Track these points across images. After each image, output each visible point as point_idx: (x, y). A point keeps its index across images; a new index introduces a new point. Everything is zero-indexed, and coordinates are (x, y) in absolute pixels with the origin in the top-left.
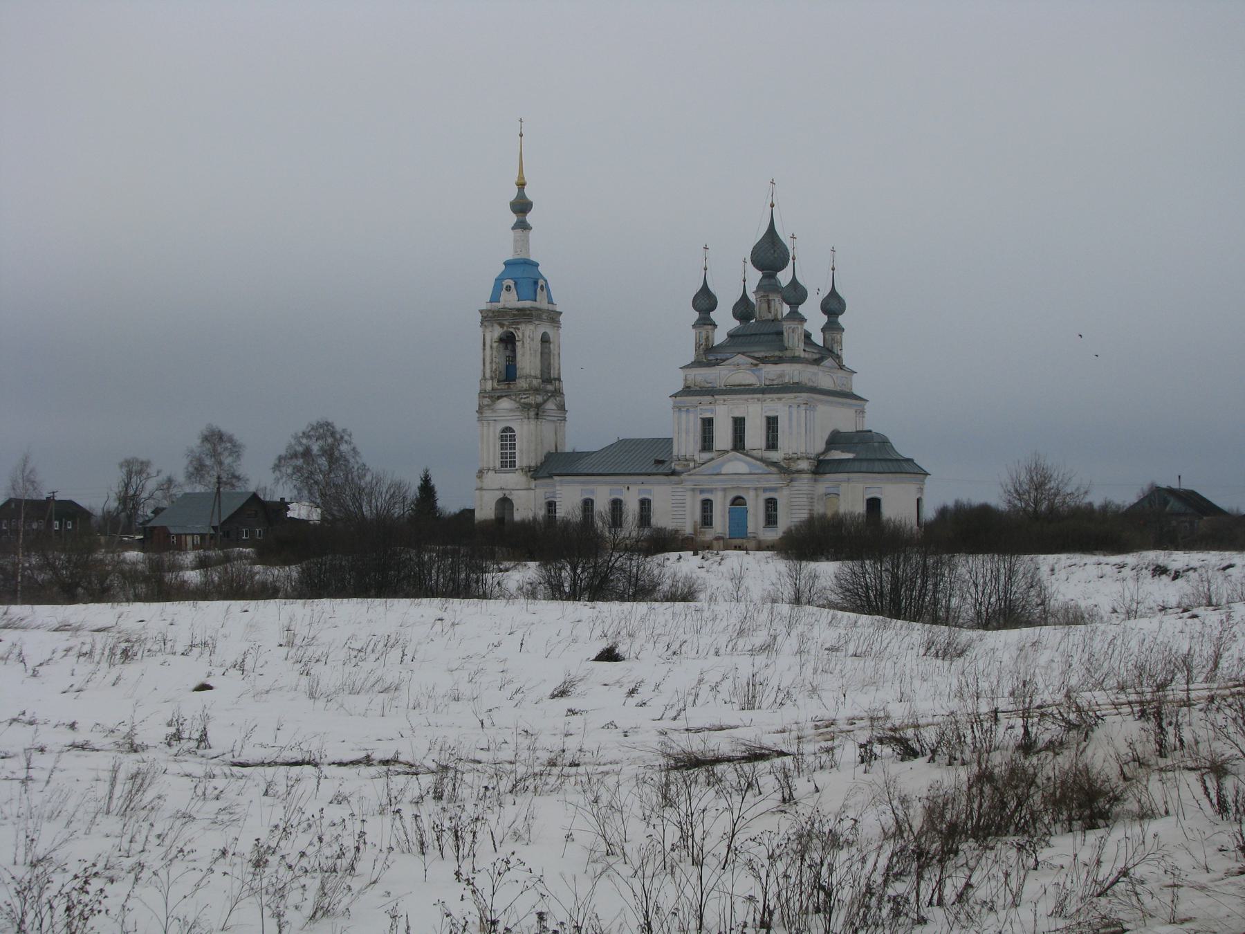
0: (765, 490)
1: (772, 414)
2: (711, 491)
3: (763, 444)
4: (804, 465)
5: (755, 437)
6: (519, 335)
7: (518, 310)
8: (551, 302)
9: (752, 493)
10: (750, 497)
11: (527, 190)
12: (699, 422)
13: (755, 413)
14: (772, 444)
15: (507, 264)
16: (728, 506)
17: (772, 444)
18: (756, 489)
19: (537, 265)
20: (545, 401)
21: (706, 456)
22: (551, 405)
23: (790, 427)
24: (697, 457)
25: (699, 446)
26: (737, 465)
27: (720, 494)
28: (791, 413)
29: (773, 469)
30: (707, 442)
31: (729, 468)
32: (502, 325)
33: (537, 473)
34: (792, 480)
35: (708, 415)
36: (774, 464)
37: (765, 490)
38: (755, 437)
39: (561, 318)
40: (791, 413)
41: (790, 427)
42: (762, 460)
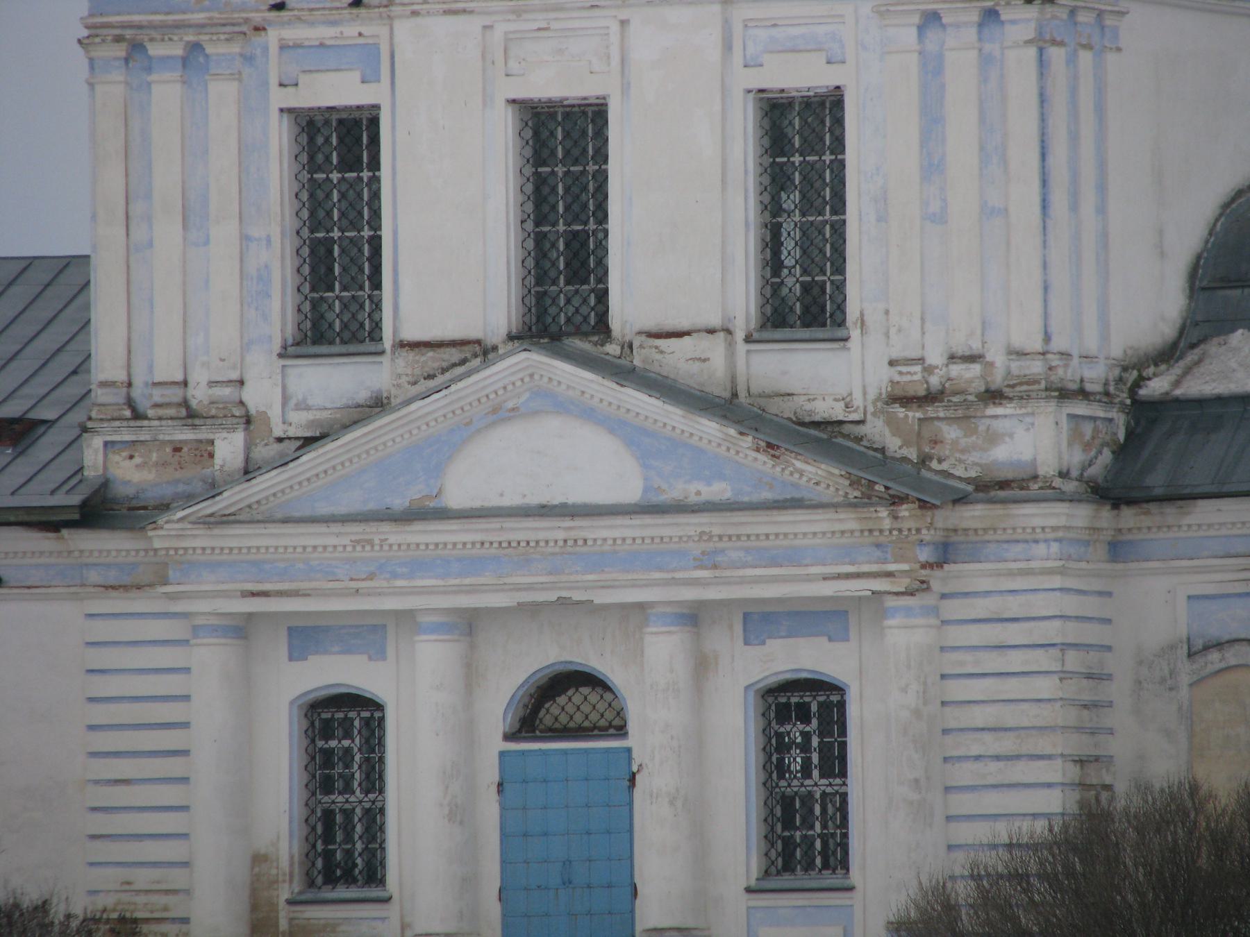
0: (761, 621)
1: (801, 76)
2: (368, 634)
3: (741, 298)
4: (1032, 439)
5: (679, 241)
9: (664, 649)
12: (278, 140)
14: (803, 294)
16: (493, 742)
17: (803, 294)
18: (693, 617)
21: (332, 381)
24: (262, 394)
25: (278, 311)
27: (433, 657)
28: (932, 68)
29: (813, 473)
30: (337, 286)
34: (945, 554)
35: (338, 90)
36: (824, 436)
37: (761, 621)
38: (679, 241)
40: (932, 68)
42: (729, 406)
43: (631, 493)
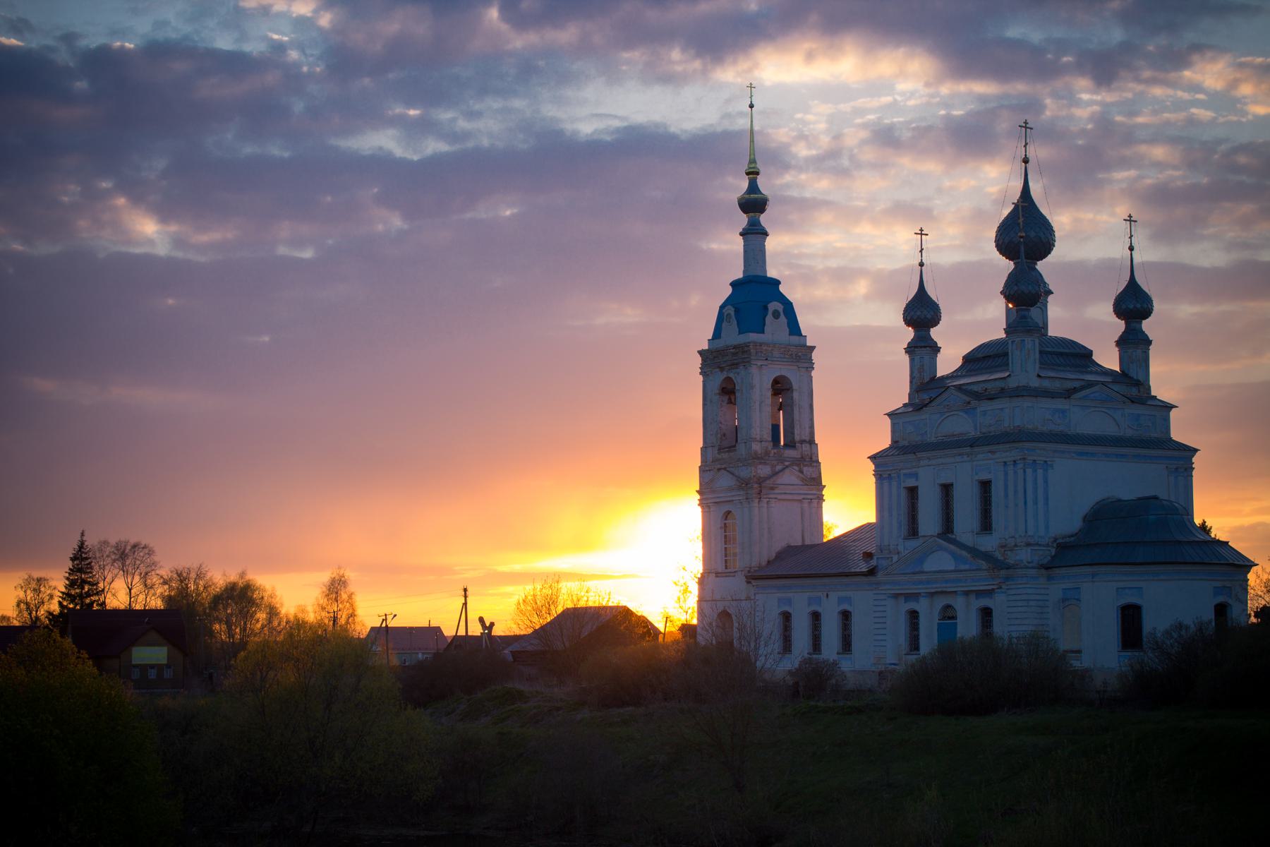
0: (980, 594)
1: (985, 476)
2: (914, 597)
4: (1024, 555)
6: (737, 380)
7: (735, 347)
8: (794, 328)
10: (959, 603)
11: (761, 182)
13: (964, 475)
14: (986, 525)
15: (734, 284)
17: (986, 525)
18: (967, 593)
19: (777, 283)
20: (775, 474)
21: (913, 544)
22: (789, 477)
23: (1006, 496)
24: (901, 548)
26: (942, 561)
28: (1006, 474)
29: (984, 564)
31: (931, 565)
32: (722, 369)
33: (754, 577)
34: (1007, 578)
36: (987, 557)
37: (980, 594)
39: (814, 355)
40: (1006, 474)
41: (1006, 496)
43: (952, 568)
